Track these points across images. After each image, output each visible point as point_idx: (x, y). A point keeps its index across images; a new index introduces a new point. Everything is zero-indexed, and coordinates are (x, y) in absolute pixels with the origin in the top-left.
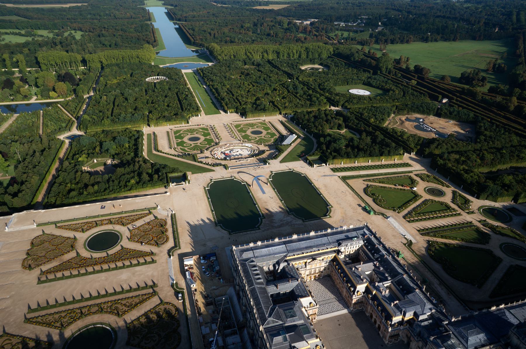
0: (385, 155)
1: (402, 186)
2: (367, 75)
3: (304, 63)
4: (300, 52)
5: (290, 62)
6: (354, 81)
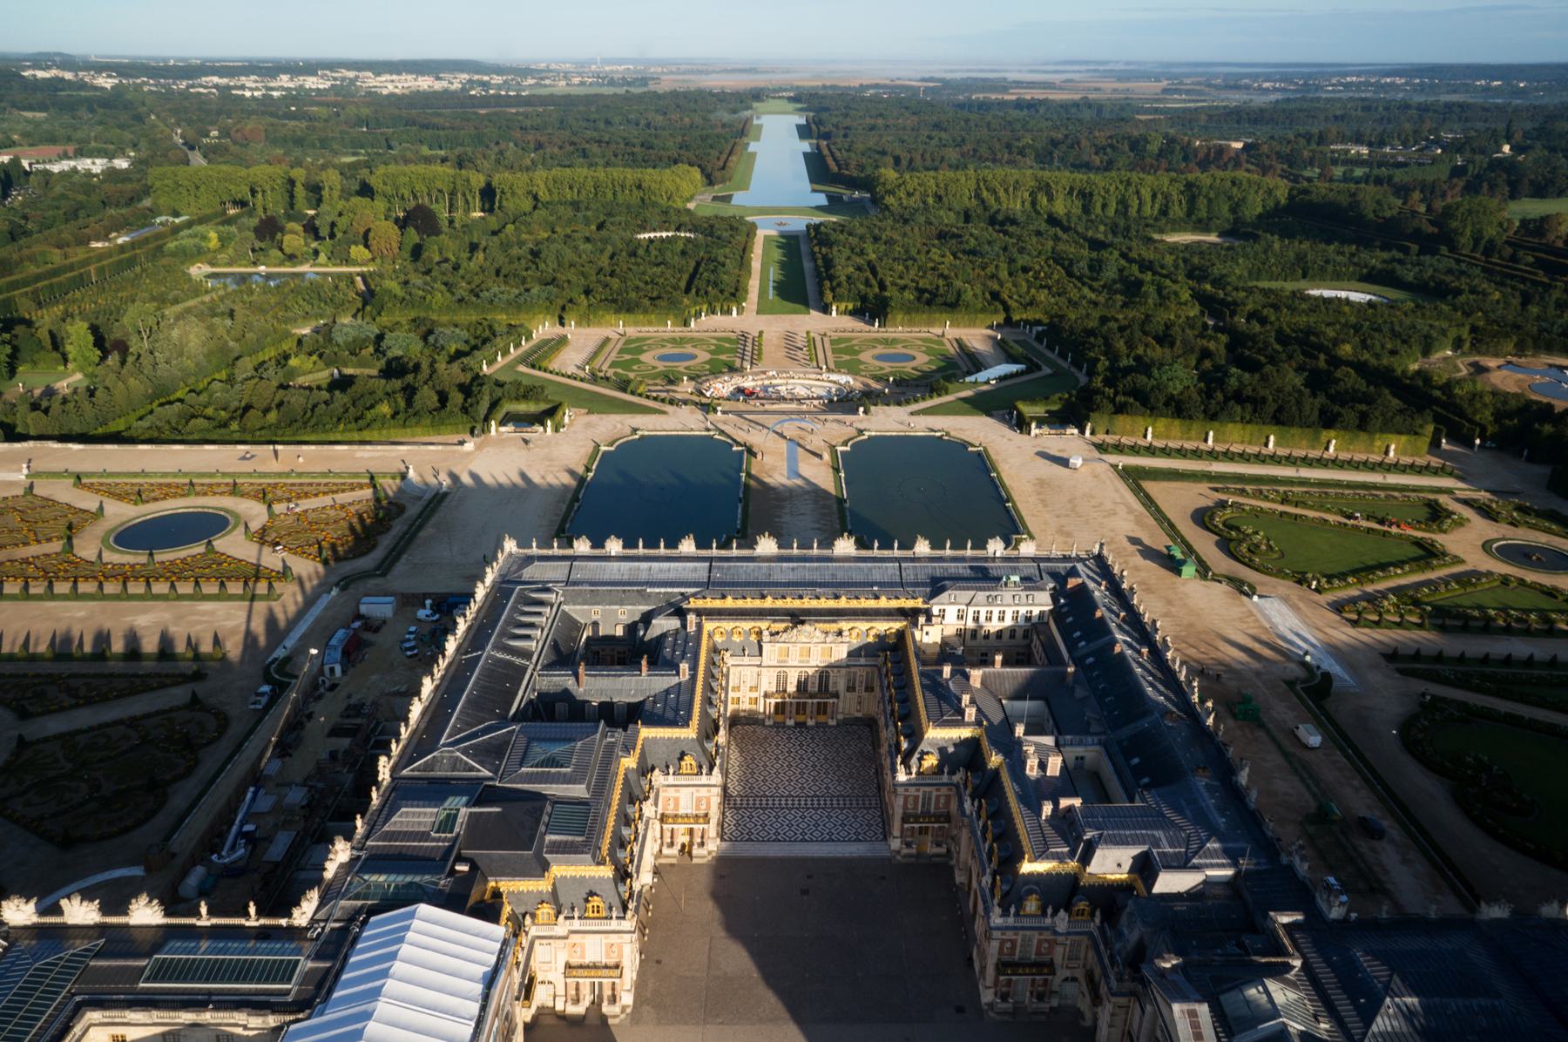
0: (1345, 428)
1: (1381, 522)
2: (1386, 255)
3: (1177, 226)
4: (1167, 197)
5: (1122, 223)
6: (1330, 268)
